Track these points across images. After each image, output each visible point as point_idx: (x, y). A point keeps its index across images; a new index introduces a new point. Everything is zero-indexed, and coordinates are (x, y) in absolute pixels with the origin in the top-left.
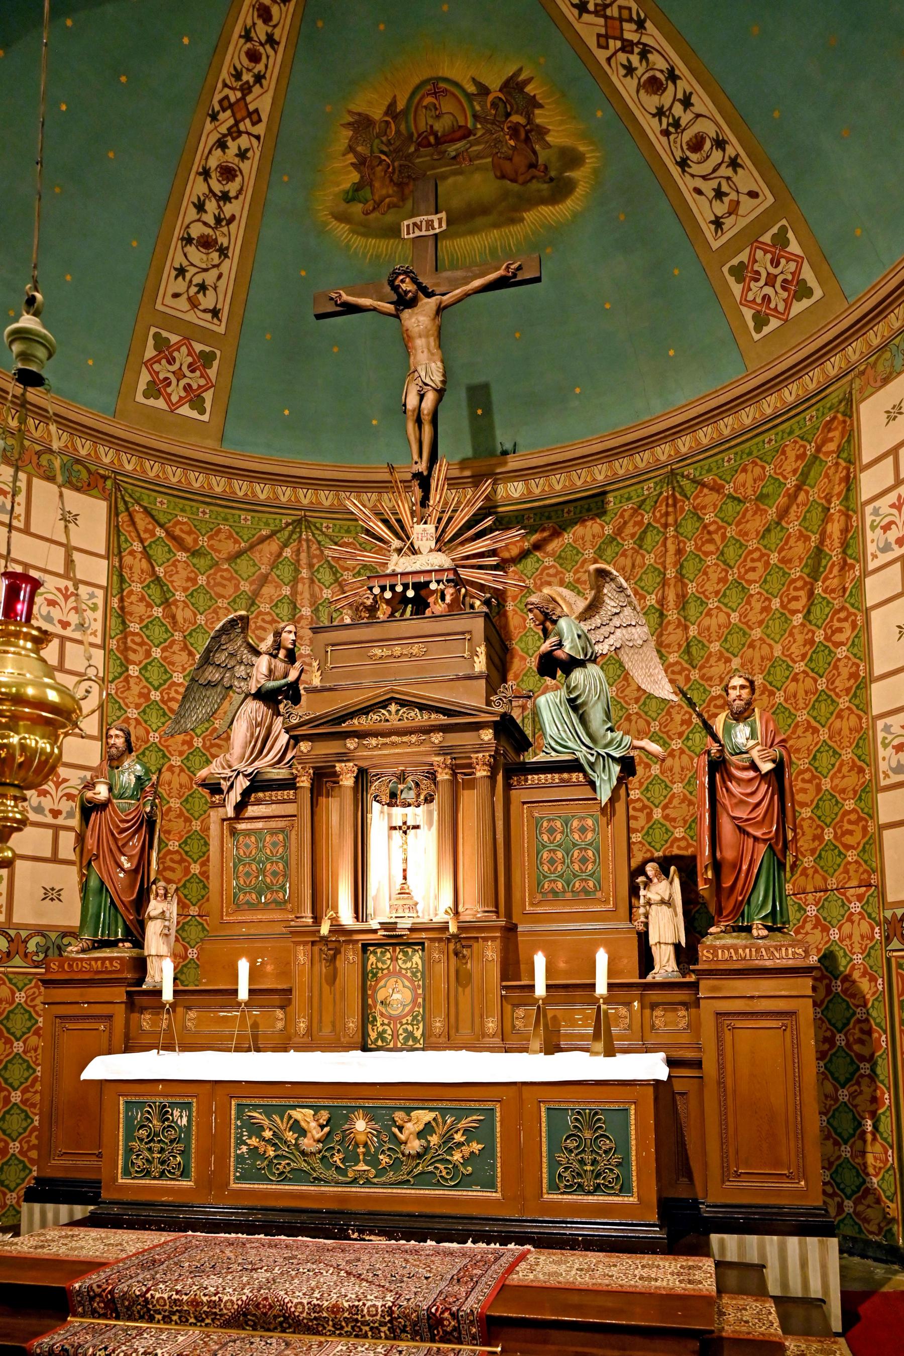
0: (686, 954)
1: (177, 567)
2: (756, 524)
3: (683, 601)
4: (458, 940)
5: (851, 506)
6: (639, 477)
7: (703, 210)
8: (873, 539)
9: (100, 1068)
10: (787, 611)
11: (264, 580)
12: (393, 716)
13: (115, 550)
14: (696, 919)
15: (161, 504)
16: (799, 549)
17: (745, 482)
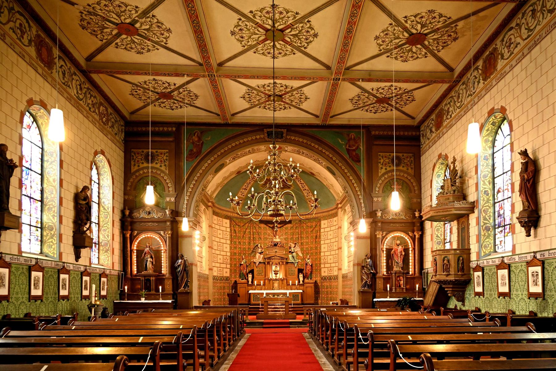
0: (303, 281)
1: (237, 228)
2: (310, 230)
3: (301, 237)
4: (282, 280)
5: (320, 232)
6: (296, 220)
7: (306, 195)
8: (322, 237)
9: (250, 292)
10: (313, 242)
11: (246, 229)
12: (276, 257)
13: (230, 227)
14: (304, 278)
15: (235, 219)
16: (314, 235)
17: (309, 224)
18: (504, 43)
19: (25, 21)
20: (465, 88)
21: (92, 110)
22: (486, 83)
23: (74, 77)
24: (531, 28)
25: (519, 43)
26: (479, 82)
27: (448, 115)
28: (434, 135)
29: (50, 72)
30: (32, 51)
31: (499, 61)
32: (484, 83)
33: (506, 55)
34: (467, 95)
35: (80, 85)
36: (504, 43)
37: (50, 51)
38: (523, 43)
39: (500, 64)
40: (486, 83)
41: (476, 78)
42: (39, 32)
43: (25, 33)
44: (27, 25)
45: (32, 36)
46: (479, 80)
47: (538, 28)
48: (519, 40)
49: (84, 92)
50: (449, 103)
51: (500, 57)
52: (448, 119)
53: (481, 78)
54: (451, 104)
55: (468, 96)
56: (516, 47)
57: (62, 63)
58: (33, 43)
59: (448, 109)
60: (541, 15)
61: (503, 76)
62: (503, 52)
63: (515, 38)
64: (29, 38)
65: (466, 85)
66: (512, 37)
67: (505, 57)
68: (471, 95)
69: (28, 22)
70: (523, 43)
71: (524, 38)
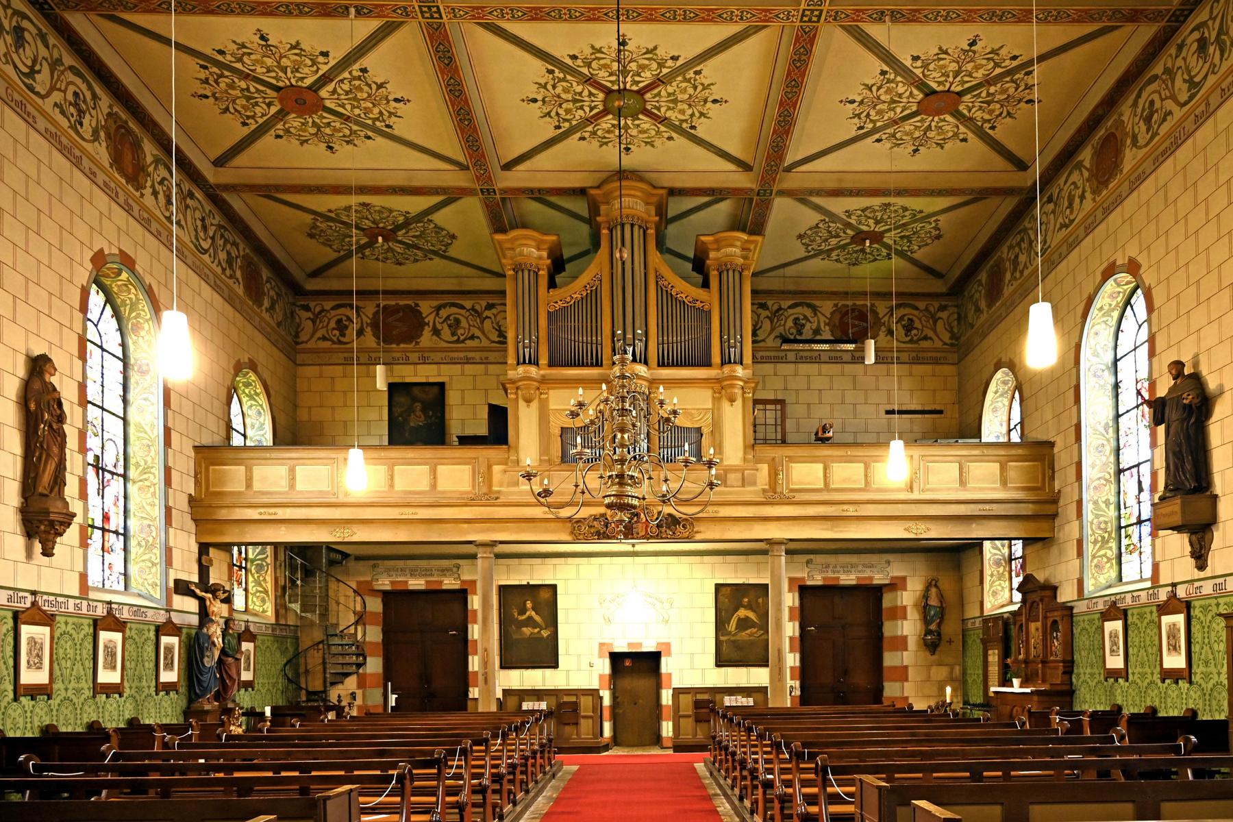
18: (1139, 110)
19: (84, 87)
20: (1053, 212)
21: (228, 272)
22: (1098, 199)
23: (189, 201)
24: (1197, 79)
25: (1170, 113)
26: (1082, 197)
27: (1015, 270)
28: (984, 317)
29: (138, 194)
30: (101, 152)
31: (1127, 151)
32: (1094, 200)
33: (1143, 137)
34: (1058, 226)
35: (203, 220)
36: (1139, 110)
37: (137, 147)
38: (1178, 113)
39: (1130, 157)
40: (1098, 199)
41: (1077, 187)
42: (115, 109)
43: (84, 113)
44: (88, 95)
45: (101, 117)
46: (1084, 191)
47: (1212, 79)
48: (1170, 105)
49: (211, 234)
50: (1019, 244)
51: (1129, 141)
52: (1016, 279)
53: (1088, 189)
54: (1023, 245)
55: (1060, 229)
56: (1164, 120)
57: (163, 172)
58: (102, 134)
59: (1017, 257)
60: (1218, 52)
61: (1137, 181)
62: (1136, 131)
63: (1162, 100)
64: (94, 125)
65: (1056, 204)
66: (1156, 97)
67: (1141, 142)
68: (1067, 226)
69: (90, 87)
70: (1178, 113)
71: (1182, 101)
